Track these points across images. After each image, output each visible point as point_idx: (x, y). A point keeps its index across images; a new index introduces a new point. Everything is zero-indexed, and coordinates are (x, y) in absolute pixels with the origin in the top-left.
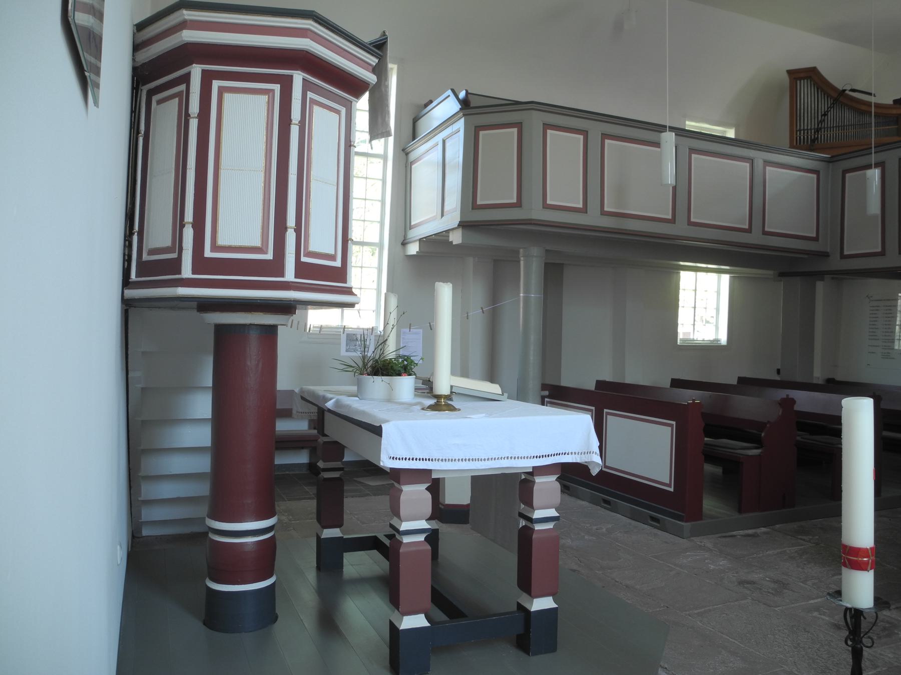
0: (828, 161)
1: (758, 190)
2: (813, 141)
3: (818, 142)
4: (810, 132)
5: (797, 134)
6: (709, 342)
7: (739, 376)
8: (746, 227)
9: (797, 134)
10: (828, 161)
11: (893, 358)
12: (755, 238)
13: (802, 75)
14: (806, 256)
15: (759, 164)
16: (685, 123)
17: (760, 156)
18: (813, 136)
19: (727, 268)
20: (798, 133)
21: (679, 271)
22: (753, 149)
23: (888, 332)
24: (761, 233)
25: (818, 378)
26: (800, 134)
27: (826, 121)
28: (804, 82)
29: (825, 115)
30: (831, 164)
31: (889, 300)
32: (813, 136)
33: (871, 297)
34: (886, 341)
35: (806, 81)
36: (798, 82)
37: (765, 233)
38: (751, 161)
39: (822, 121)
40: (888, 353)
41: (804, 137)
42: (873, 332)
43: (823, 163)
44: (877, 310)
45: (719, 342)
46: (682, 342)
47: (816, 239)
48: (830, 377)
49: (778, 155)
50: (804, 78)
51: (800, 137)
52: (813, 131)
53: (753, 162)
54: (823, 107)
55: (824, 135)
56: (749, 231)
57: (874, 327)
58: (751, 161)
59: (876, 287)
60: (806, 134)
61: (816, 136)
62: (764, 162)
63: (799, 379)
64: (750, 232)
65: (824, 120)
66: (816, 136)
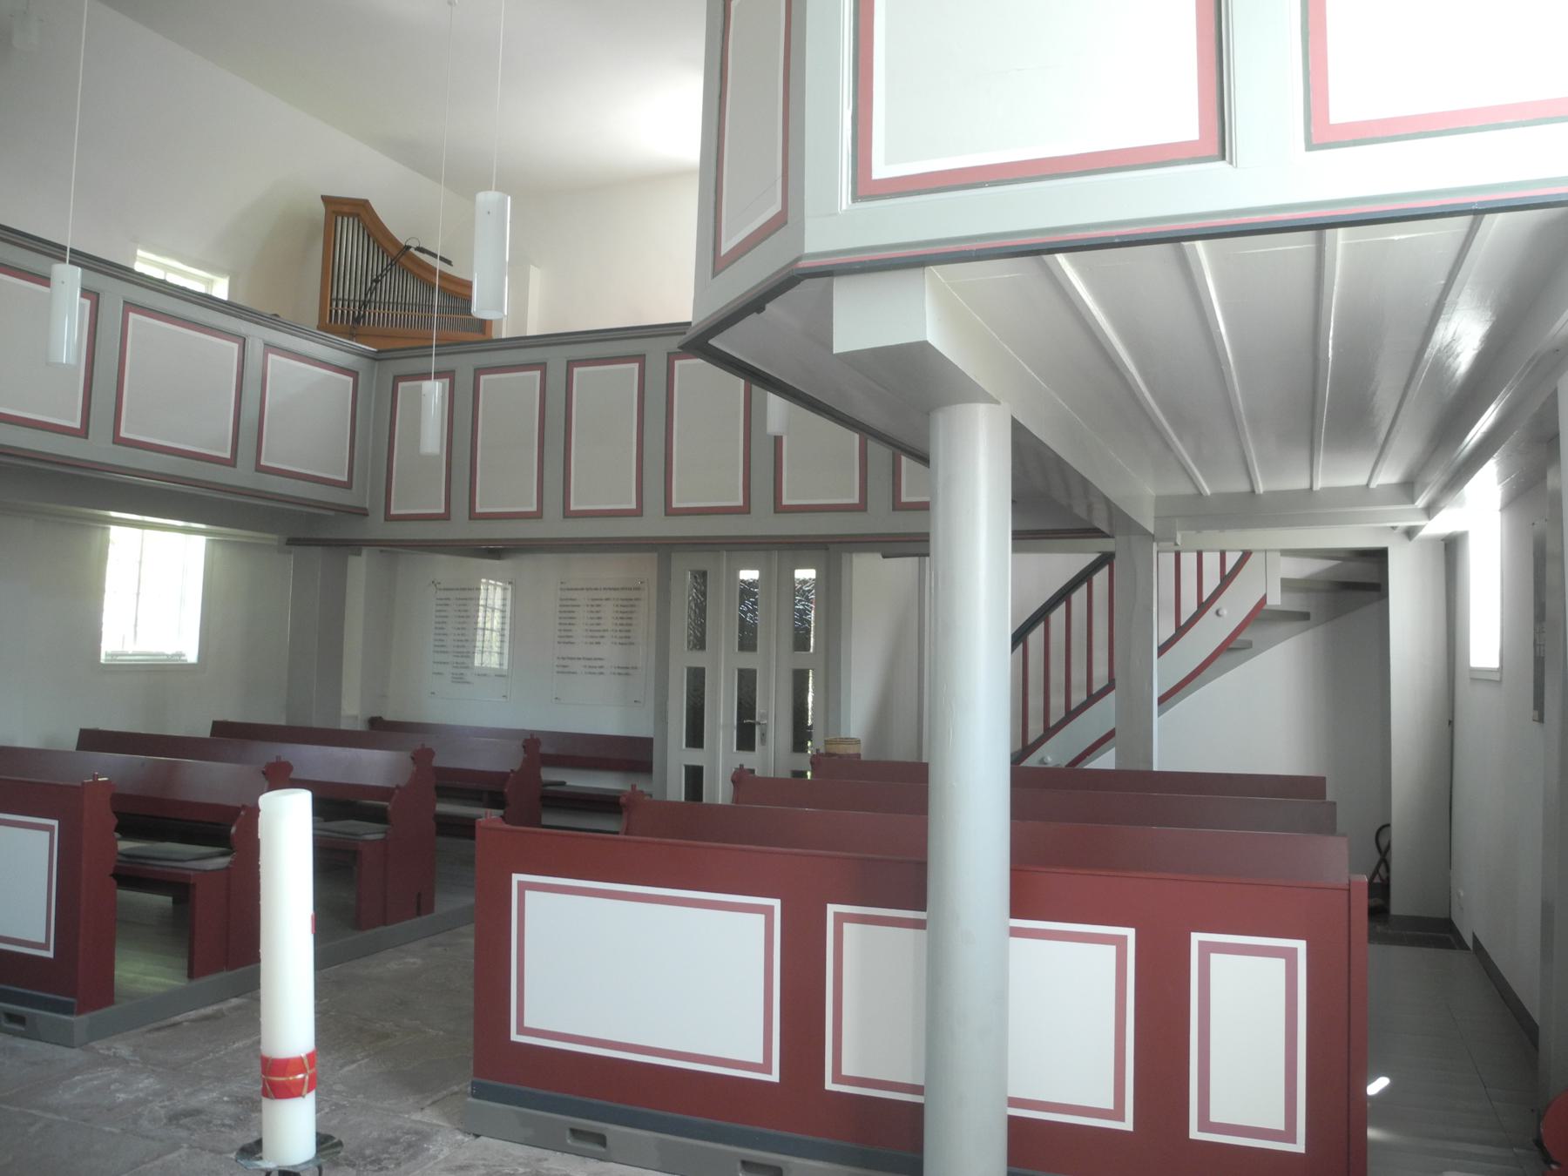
0: (375, 358)
1: (251, 393)
2: (357, 320)
3: (364, 323)
4: (352, 305)
5: (331, 305)
6: (165, 657)
7: (219, 718)
8: (227, 455)
9: (331, 305)
10: (375, 358)
11: (468, 683)
12: (240, 475)
13: (346, 209)
14: (332, 513)
15: (255, 349)
16: (136, 252)
17: (258, 335)
18: (357, 313)
19: (202, 526)
20: (334, 304)
21: (108, 526)
22: (245, 319)
23: (461, 641)
24: (253, 469)
25: (356, 718)
26: (337, 305)
27: (379, 291)
28: (342, 219)
29: (376, 281)
30: (377, 363)
31: (464, 589)
32: (357, 313)
33: (439, 583)
34: (459, 655)
35: (351, 219)
36: (340, 219)
37: (260, 469)
38: (241, 341)
39: (372, 290)
40: (462, 674)
41: (342, 312)
42: (440, 640)
43: (366, 360)
44: (447, 605)
45: (183, 658)
46: (109, 658)
47: (347, 485)
48: (375, 715)
49: (290, 336)
50: (349, 215)
51: (336, 312)
52: (357, 304)
53: (245, 342)
54: (376, 266)
55: (374, 314)
56: (232, 462)
57: (441, 631)
58: (243, 341)
59: (446, 568)
60: (346, 307)
61: (362, 313)
62: (265, 344)
63: (316, 721)
64: (234, 466)
65: (376, 288)
66: (362, 313)
